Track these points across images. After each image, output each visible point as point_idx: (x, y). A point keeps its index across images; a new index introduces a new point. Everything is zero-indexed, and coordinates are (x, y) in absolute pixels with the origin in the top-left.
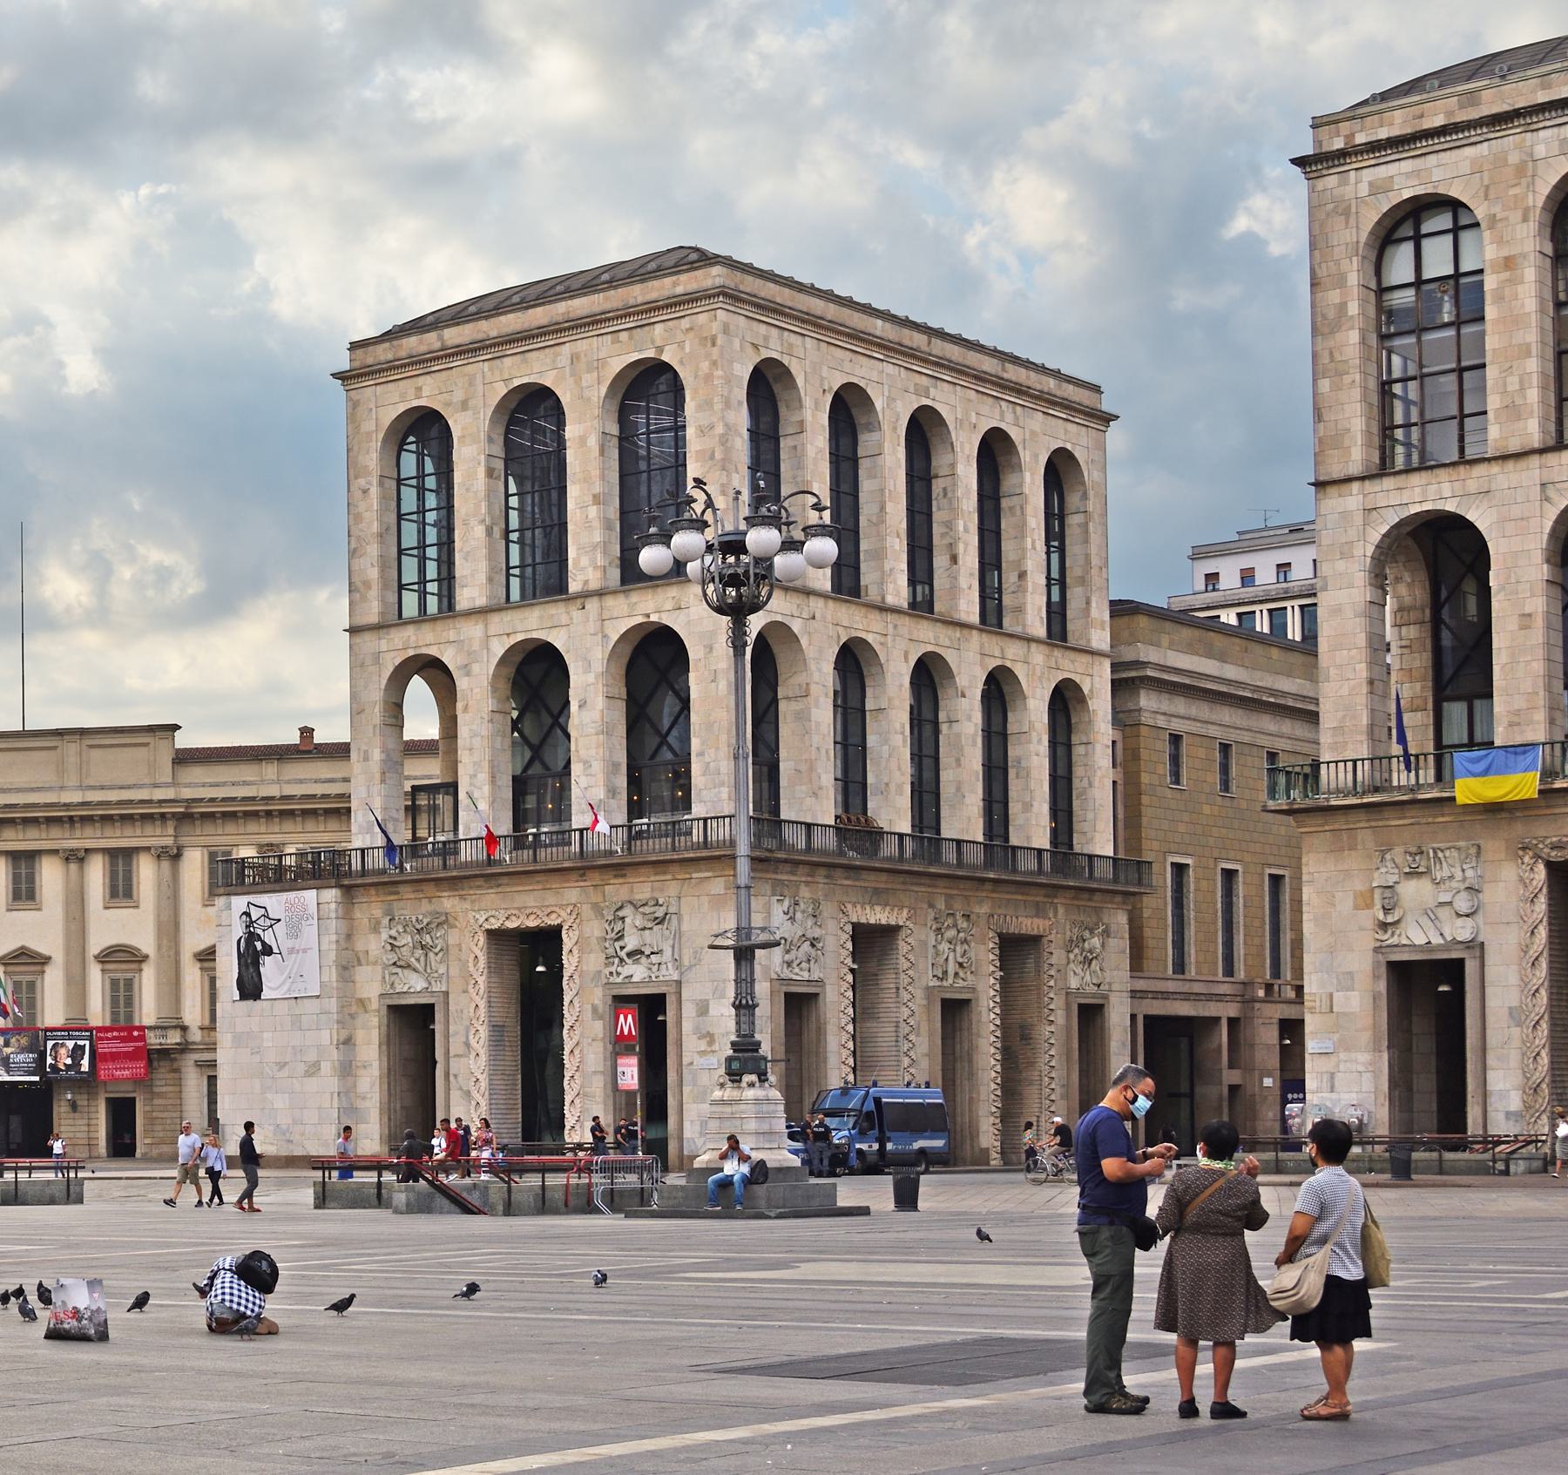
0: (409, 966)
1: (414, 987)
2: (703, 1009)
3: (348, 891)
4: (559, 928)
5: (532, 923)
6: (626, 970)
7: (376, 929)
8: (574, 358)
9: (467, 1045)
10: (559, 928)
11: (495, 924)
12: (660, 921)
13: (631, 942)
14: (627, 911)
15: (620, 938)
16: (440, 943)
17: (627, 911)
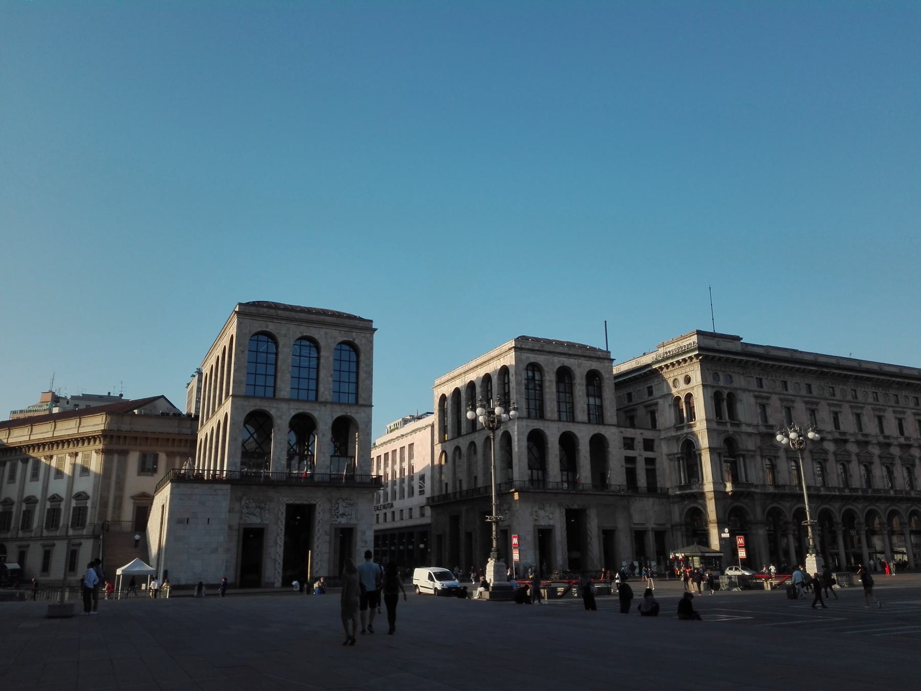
0: (254, 515)
1: (255, 521)
2: (364, 533)
3: (232, 485)
4: (315, 505)
5: (305, 502)
6: (339, 520)
7: (239, 500)
8: (326, 333)
9: (276, 543)
10: (315, 505)
11: (291, 502)
12: (352, 505)
13: (341, 511)
14: (340, 501)
15: (337, 509)
16: (267, 507)
17: (340, 501)
